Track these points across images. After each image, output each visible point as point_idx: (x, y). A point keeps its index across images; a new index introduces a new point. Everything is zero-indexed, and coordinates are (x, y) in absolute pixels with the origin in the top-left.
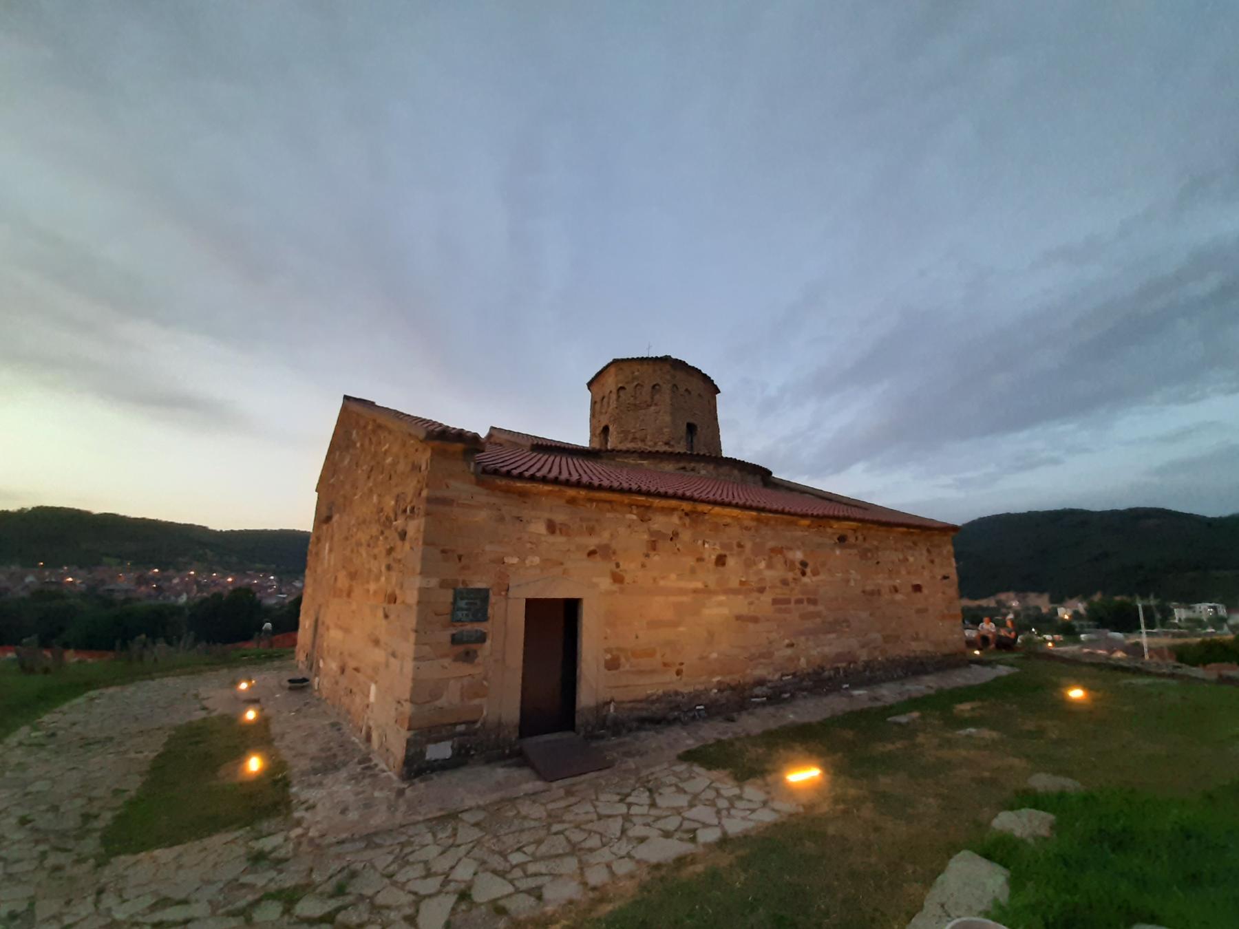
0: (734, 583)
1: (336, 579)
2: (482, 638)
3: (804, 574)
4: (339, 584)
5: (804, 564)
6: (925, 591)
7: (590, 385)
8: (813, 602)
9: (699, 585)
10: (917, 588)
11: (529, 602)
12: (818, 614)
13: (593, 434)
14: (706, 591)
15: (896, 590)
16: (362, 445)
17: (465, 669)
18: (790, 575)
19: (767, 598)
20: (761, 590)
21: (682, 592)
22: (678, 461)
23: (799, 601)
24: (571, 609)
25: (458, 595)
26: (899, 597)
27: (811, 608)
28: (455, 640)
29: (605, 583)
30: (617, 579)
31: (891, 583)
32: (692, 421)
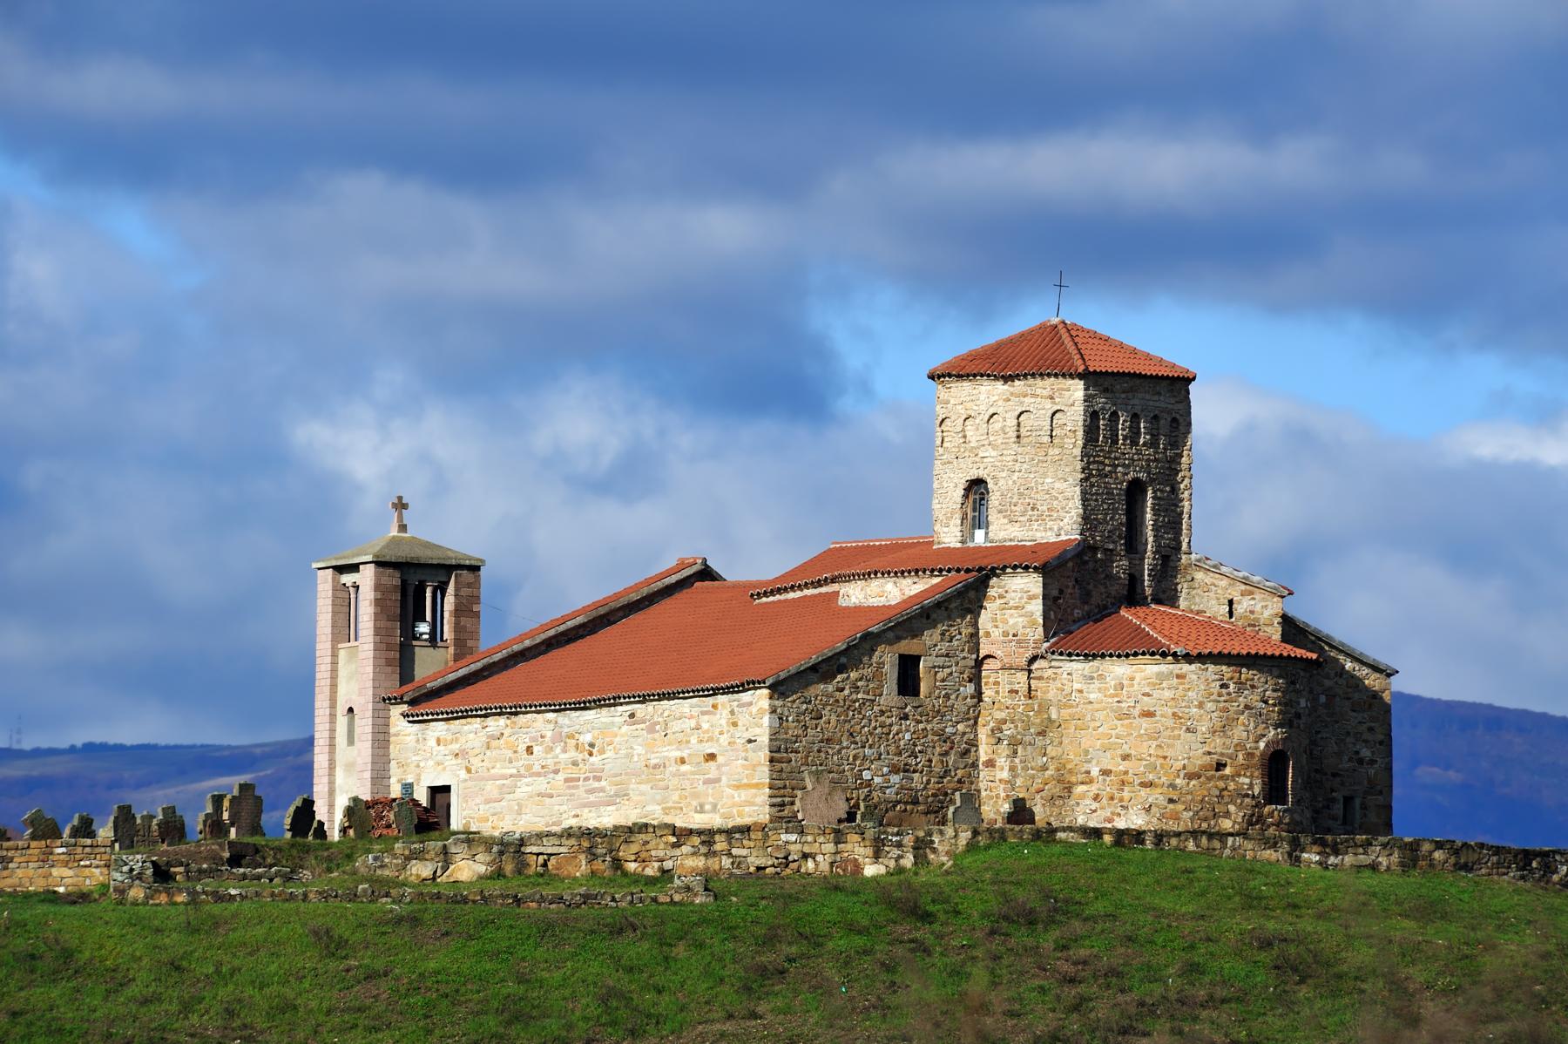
3: (591, 754)
5: (592, 745)
6: (720, 759)
8: (598, 779)
9: (514, 771)
10: (711, 757)
12: (602, 790)
14: (520, 775)
15: (683, 761)
19: (561, 777)
20: (556, 772)
21: (504, 777)
23: (586, 779)
26: (684, 768)
27: (596, 784)
29: (463, 774)
30: (469, 771)
31: (678, 754)
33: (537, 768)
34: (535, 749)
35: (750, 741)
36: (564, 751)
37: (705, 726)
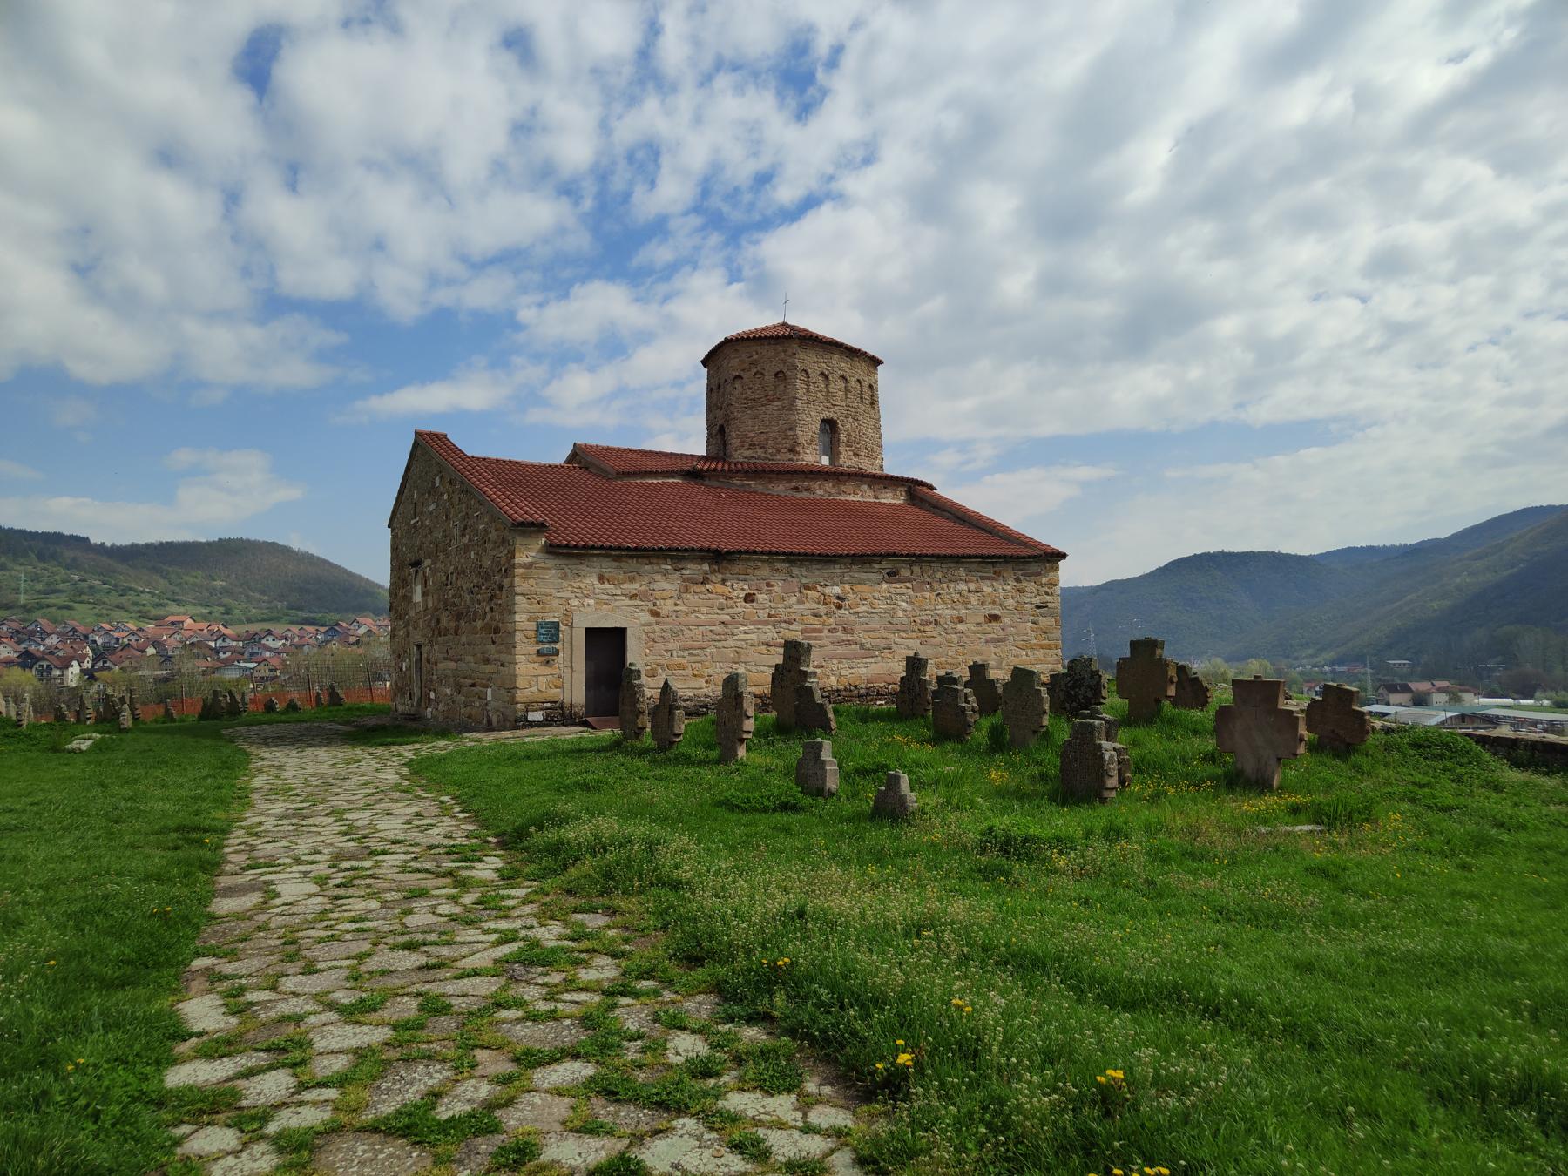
0: (763, 614)
1: (438, 621)
2: (557, 653)
3: (839, 607)
4: (444, 621)
6: (1007, 620)
7: (705, 362)
11: (590, 632)
13: (710, 435)
15: (961, 620)
16: (450, 499)
17: (547, 670)
18: (822, 609)
22: (790, 481)
24: (620, 633)
25: (538, 624)
26: (961, 627)
28: (539, 653)
29: (646, 617)
30: (655, 614)
32: (827, 415)
33: (763, 614)
34: (760, 597)
35: (1038, 607)
36: (800, 602)
37: (988, 590)
